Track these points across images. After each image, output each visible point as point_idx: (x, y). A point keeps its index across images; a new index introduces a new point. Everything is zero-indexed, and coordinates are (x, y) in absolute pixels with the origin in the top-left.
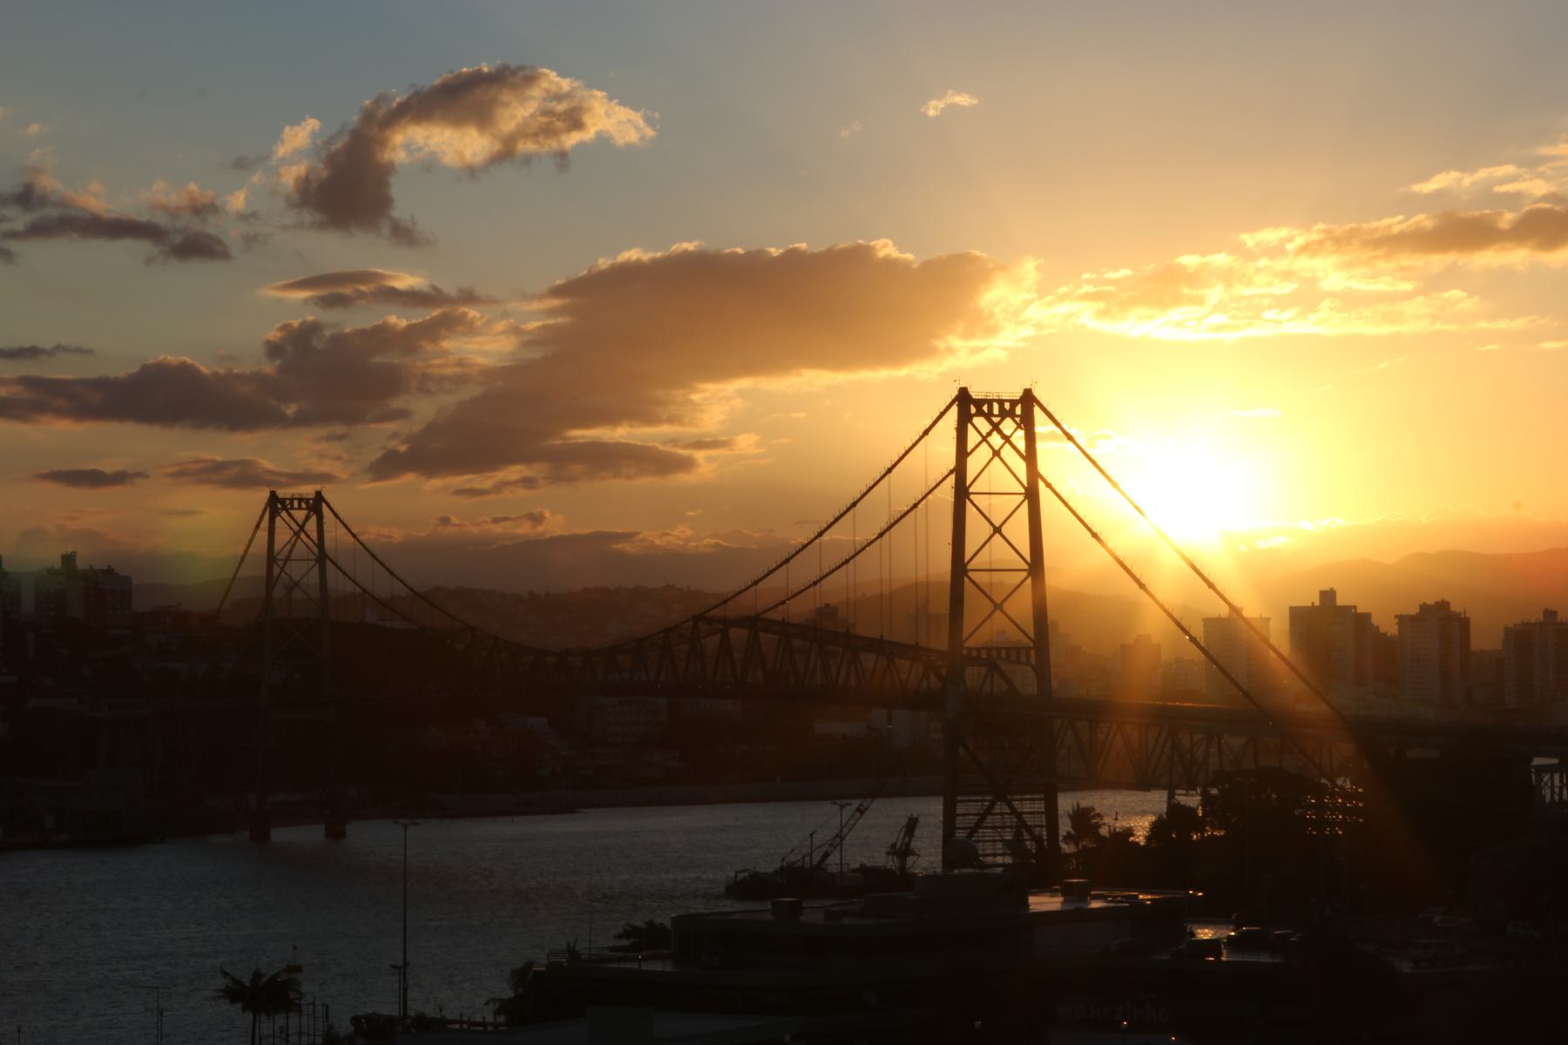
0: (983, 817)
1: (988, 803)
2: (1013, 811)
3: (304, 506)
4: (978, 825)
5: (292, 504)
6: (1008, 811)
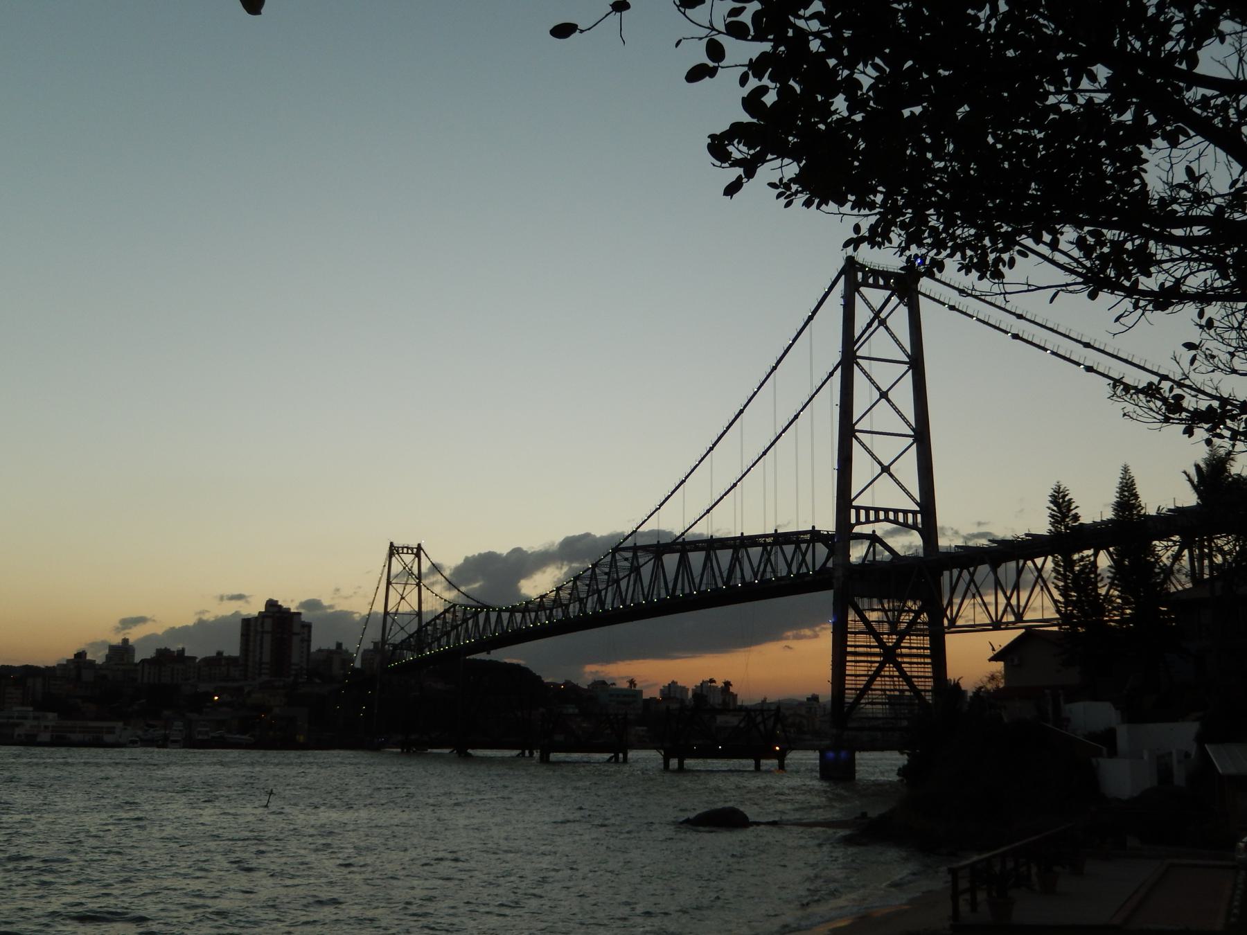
0: (872, 678)
1: (877, 665)
2: (903, 674)
3: (410, 552)
4: (868, 686)
5: (403, 550)
6: (897, 674)
